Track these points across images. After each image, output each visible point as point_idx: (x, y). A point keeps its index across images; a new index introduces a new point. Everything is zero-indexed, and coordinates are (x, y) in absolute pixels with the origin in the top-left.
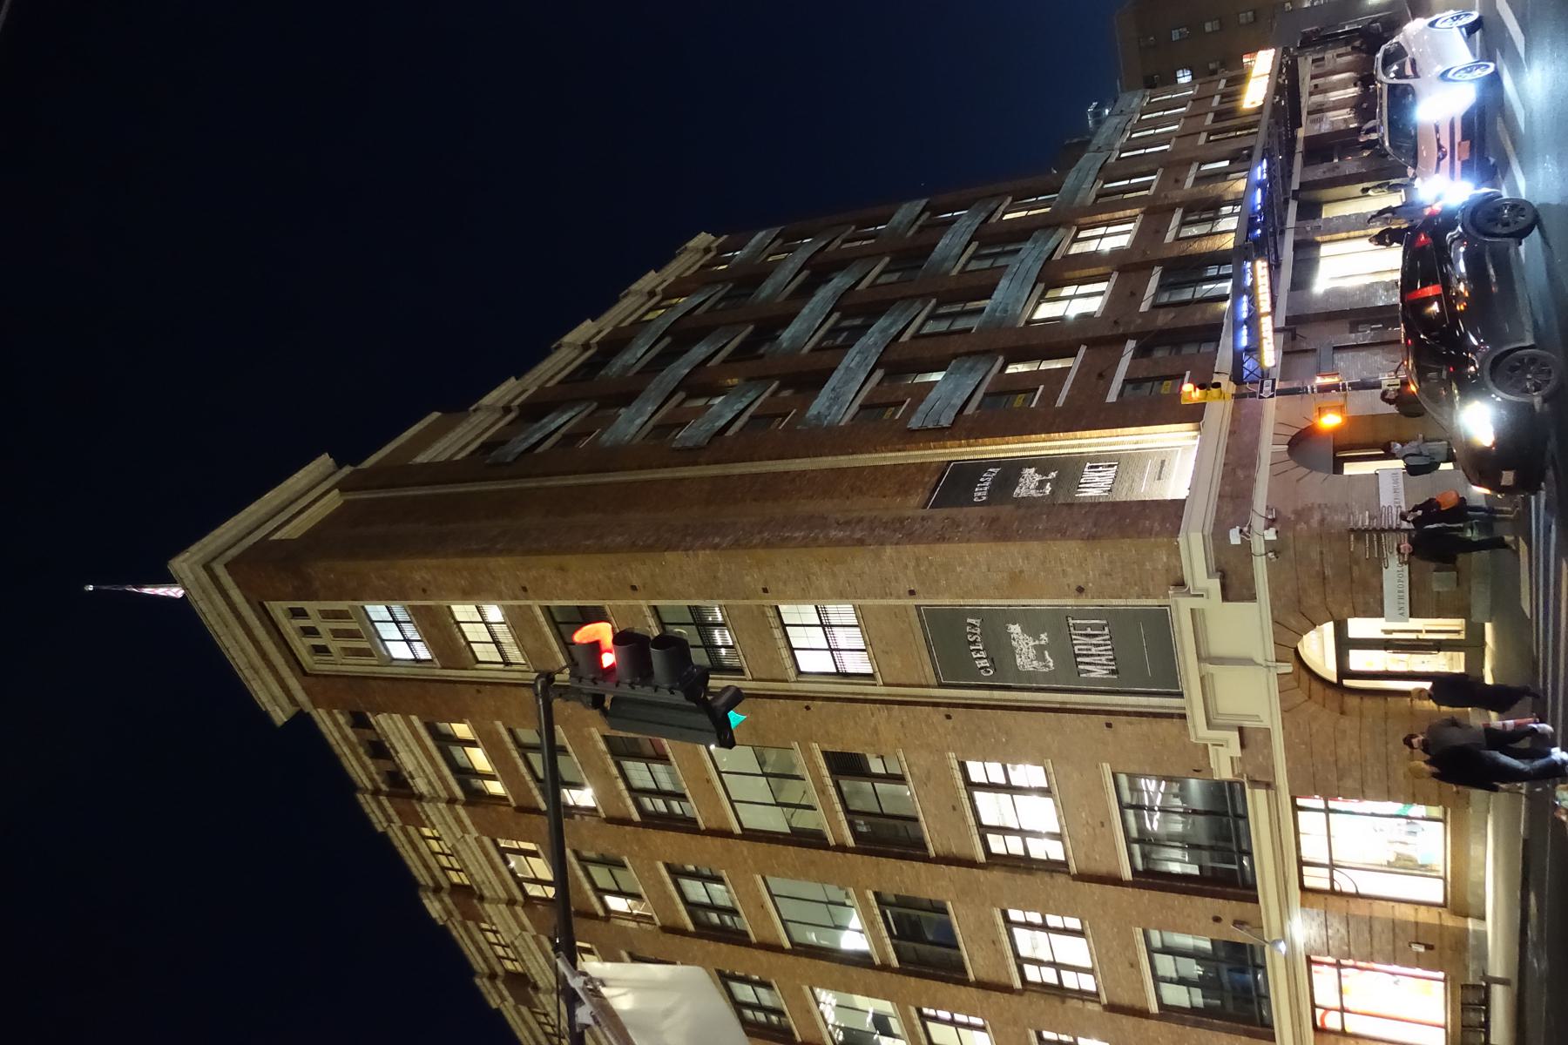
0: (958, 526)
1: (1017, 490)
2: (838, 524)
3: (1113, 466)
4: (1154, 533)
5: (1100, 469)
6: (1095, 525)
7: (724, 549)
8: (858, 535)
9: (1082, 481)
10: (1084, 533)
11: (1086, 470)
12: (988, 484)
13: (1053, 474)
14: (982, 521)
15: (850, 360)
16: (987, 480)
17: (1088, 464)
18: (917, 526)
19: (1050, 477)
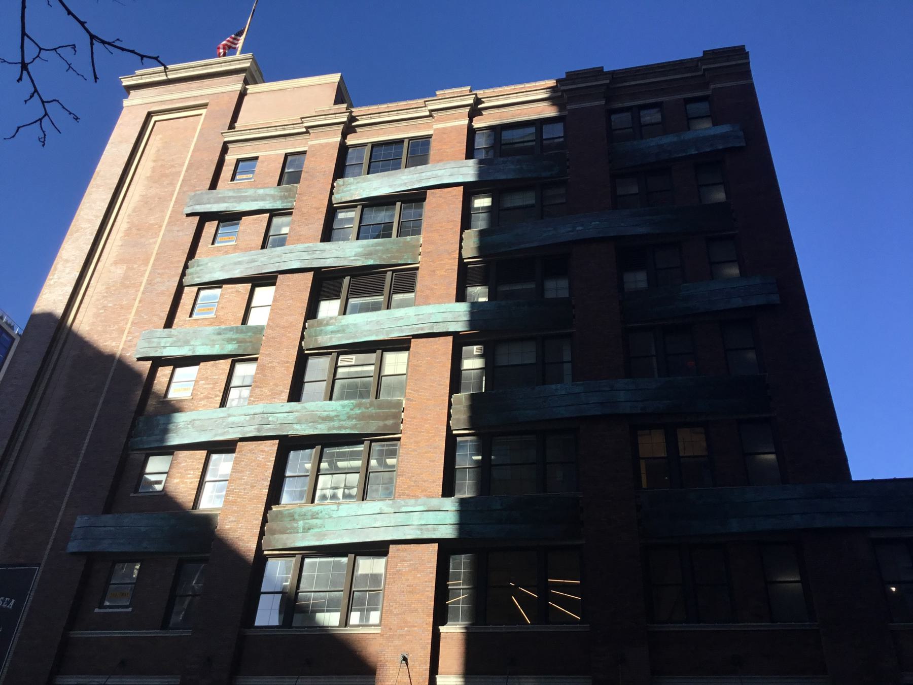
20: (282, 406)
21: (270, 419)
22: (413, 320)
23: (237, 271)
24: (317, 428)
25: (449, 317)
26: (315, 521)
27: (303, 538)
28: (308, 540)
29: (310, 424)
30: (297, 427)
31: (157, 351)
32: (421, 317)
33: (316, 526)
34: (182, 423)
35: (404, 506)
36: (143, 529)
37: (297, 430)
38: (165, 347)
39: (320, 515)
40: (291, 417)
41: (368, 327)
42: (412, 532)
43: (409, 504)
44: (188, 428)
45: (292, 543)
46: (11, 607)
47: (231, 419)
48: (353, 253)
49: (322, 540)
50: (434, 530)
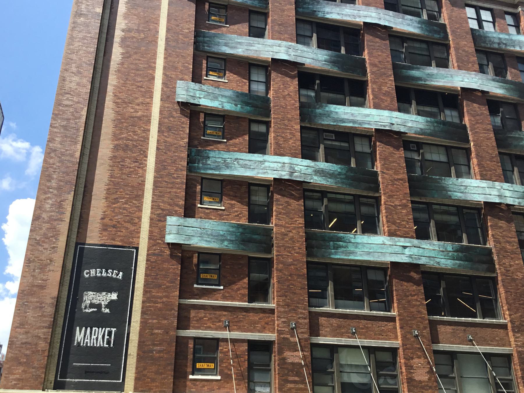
0: (41, 269)
1: (91, 293)
2: (60, 201)
3: (109, 342)
4: (7, 376)
5: (106, 337)
6: (22, 343)
7: (47, 145)
8: (44, 215)
9: (94, 329)
10: (16, 338)
11: (107, 329)
12: (104, 274)
13: (107, 311)
14: (43, 280)
15: (275, 160)
16: (112, 274)
17: (114, 330)
18: (46, 246)
19: (103, 309)
20: (302, 161)
21: (296, 169)
22: (377, 119)
23: (240, 50)
24: (328, 181)
25: (399, 121)
26: (341, 243)
27: (336, 253)
28: (339, 255)
29: (323, 177)
30: (315, 178)
31: (194, 99)
32: (381, 117)
33: (342, 247)
34: (229, 160)
35: (397, 241)
36: (221, 233)
37: (316, 180)
38: (200, 98)
39: (343, 239)
40: (310, 171)
41: (346, 117)
42: (407, 258)
43: (400, 241)
44: (235, 164)
45: (328, 255)
46: (120, 278)
47: (267, 164)
48: (324, 59)
49: (349, 256)
50: (419, 259)
